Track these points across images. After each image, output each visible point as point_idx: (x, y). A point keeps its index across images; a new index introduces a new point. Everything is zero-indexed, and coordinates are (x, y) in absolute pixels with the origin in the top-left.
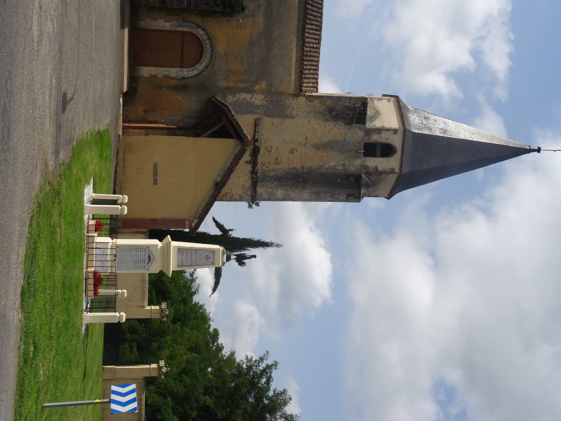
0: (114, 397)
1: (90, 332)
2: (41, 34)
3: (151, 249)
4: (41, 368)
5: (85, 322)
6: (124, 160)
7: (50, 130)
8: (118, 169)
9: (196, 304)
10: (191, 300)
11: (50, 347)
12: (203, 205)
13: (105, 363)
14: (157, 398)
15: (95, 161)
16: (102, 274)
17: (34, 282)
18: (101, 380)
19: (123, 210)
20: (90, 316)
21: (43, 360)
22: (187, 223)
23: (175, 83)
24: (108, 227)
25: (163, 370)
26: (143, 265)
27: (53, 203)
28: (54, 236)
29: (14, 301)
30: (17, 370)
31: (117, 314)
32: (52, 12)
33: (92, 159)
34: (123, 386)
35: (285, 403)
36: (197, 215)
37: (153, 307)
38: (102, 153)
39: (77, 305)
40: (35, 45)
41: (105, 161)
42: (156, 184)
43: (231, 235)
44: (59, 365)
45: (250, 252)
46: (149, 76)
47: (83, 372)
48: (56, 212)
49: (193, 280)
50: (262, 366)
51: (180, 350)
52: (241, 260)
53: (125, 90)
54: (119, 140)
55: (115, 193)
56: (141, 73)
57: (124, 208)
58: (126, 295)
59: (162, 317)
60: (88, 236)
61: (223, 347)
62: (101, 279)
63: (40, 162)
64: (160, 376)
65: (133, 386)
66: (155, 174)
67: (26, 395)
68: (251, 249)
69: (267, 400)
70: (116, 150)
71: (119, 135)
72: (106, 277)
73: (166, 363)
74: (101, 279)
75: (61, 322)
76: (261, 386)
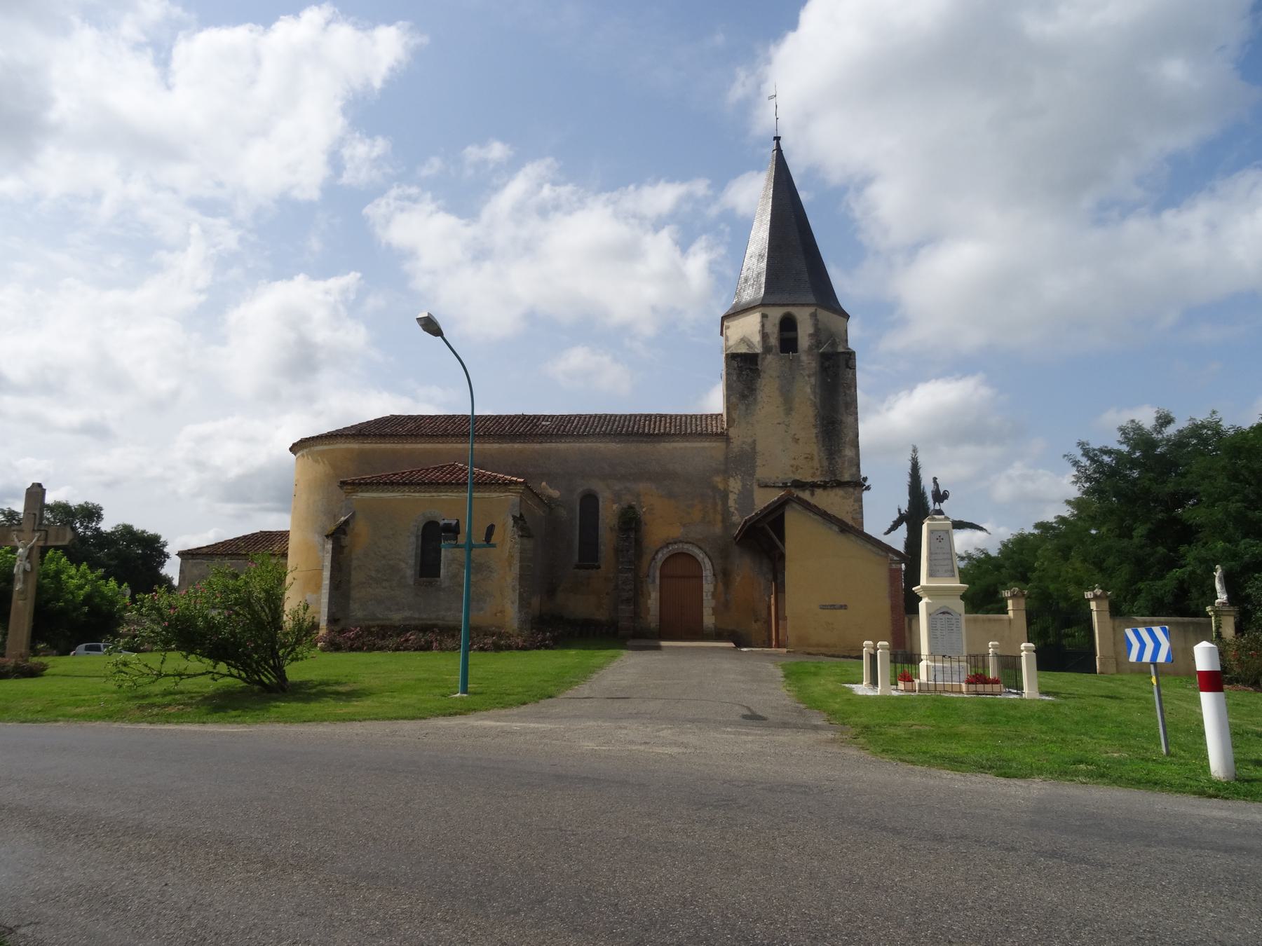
0: (1147, 658)
1: (1051, 690)
2: (675, 744)
3: (932, 611)
4: (1109, 754)
5: (1037, 696)
6: (818, 645)
7: (789, 735)
8: (830, 654)
9: (1001, 552)
10: (994, 558)
11: (1077, 743)
12: (869, 546)
13: (1092, 670)
14: (1141, 602)
15: (823, 682)
16: (969, 674)
17: (987, 760)
18: (1118, 676)
19: (883, 647)
20: (1029, 690)
21: (1098, 752)
22: (894, 566)
23: (720, 585)
24: (906, 665)
25: (1099, 593)
26: (954, 621)
27: (881, 734)
28: (923, 733)
29: (1018, 788)
30: (1116, 787)
31: (1023, 654)
32: (648, 729)
33: (820, 685)
34: (1130, 645)
35: (1138, 429)
36: (883, 554)
37: (1010, 607)
38: (811, 673)
39: (1013, 705)
40: (689, 751)
41: (820, 669)
42: (846, 606)
43: (906, 511)
44: (1102, 731)
45: (927, 486)
46: (714, 617)
47: (1108, 699)
48: (892, 731)
49: (969, 557)
50: (1085, 462)
51: (1067, 572)
52: (940, 497)
53: (733, 645)
54: (794, 652)
55: (861, 658)
56: (711, 626)
57: (880, 645)
58: (996, 643)
59: (1024, 595)
60: (920, 691)
61: (1059, 516)
62: (977, 674)
63: (829, 749)
64: (1107, 597)
65: (1129, 632)
66: (833, 607)
67: (1152, 777)
68: (922, 484)
69: (1135, 453)
70: (805, 656)
71: (787, 652)
72: (973, 669)
73: (1088, 590)
74: (977, 674)
75: (1039, 727)
76: (1114, 462)
